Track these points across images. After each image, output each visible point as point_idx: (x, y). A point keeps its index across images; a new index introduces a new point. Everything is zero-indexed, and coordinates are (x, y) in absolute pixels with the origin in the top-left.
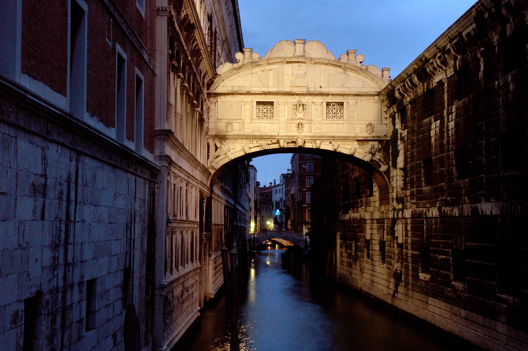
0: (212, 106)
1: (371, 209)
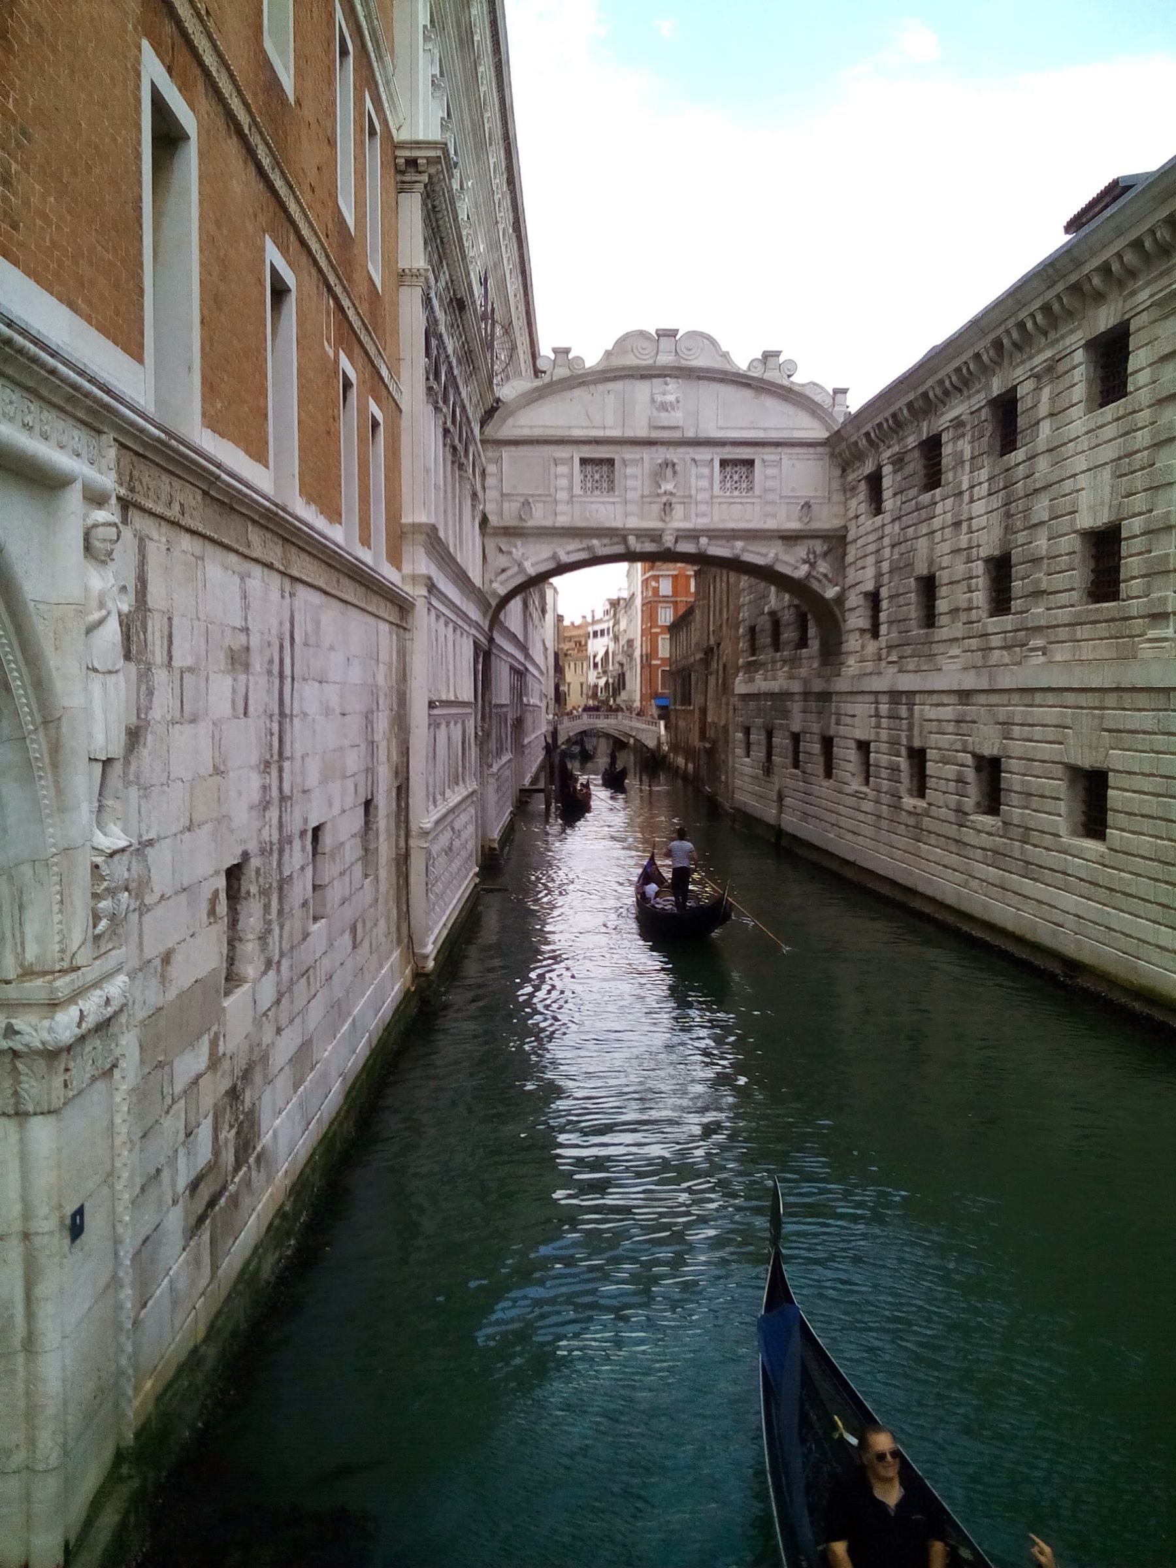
0: (491, 469)
1: (803, 672)
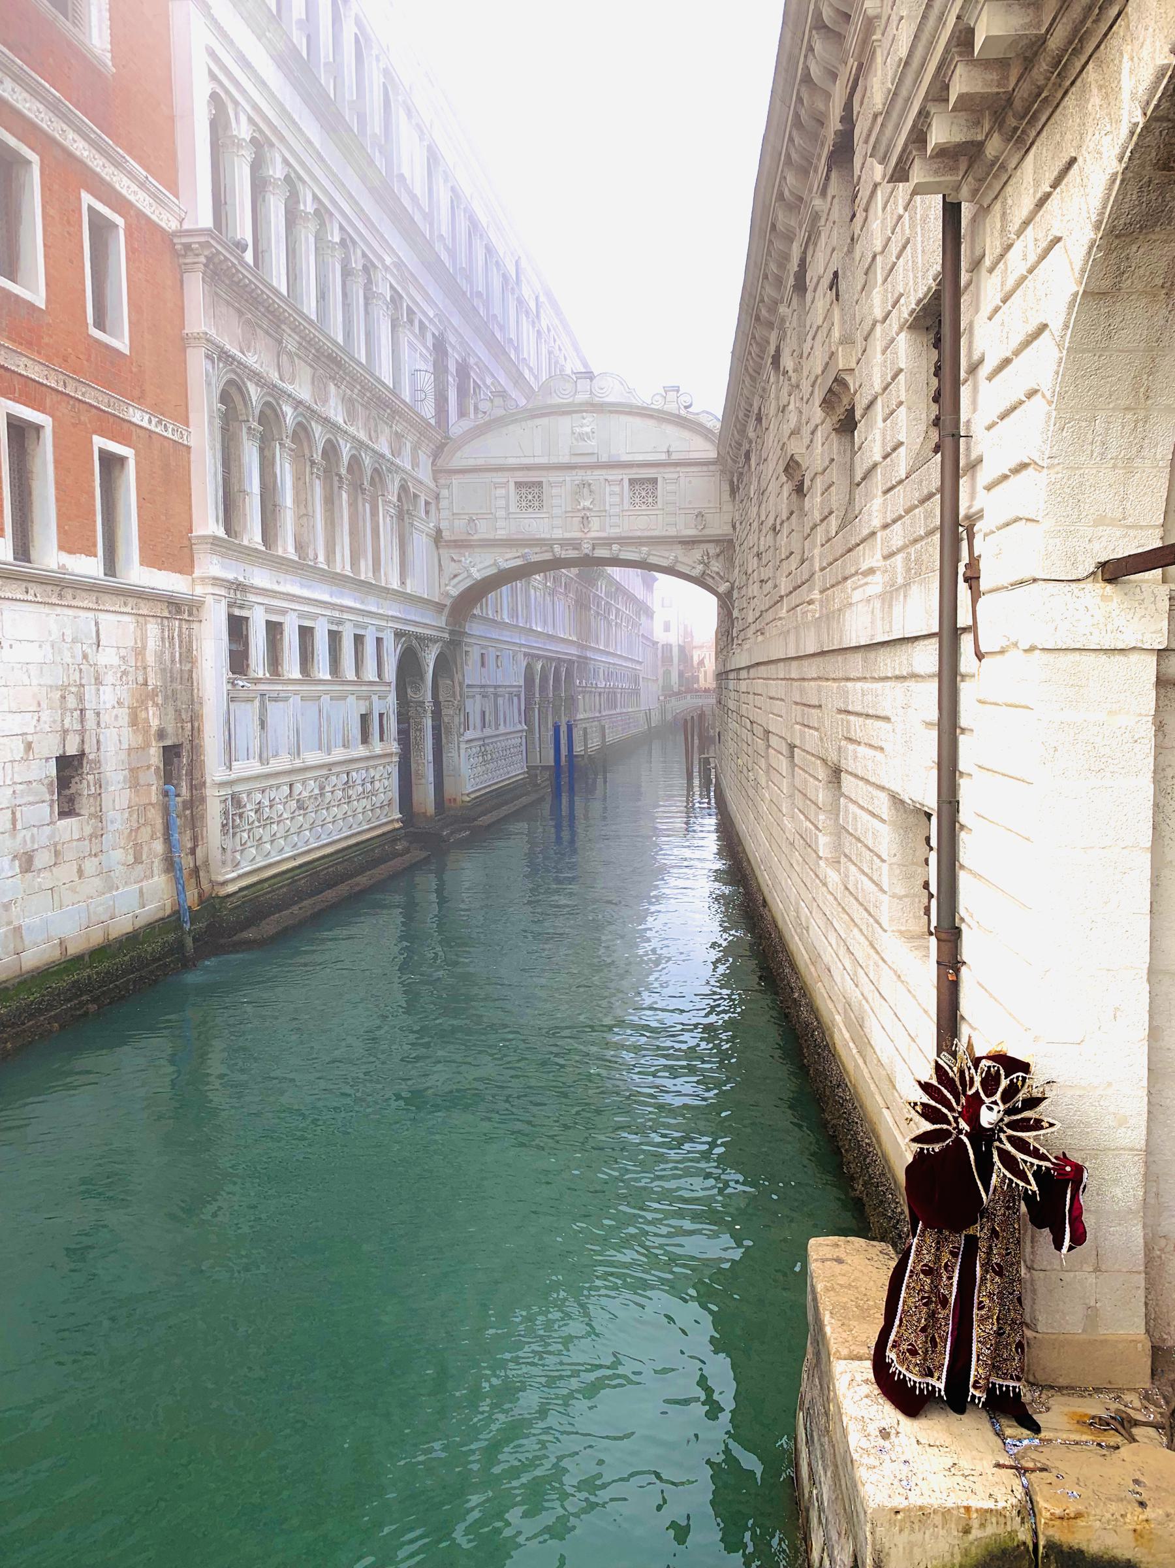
0: (444, 493)
